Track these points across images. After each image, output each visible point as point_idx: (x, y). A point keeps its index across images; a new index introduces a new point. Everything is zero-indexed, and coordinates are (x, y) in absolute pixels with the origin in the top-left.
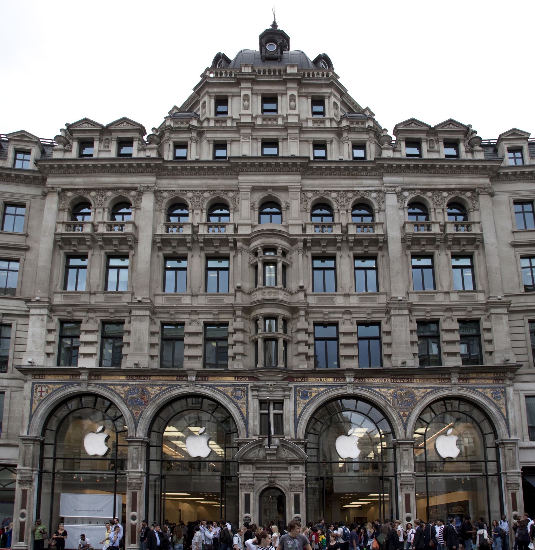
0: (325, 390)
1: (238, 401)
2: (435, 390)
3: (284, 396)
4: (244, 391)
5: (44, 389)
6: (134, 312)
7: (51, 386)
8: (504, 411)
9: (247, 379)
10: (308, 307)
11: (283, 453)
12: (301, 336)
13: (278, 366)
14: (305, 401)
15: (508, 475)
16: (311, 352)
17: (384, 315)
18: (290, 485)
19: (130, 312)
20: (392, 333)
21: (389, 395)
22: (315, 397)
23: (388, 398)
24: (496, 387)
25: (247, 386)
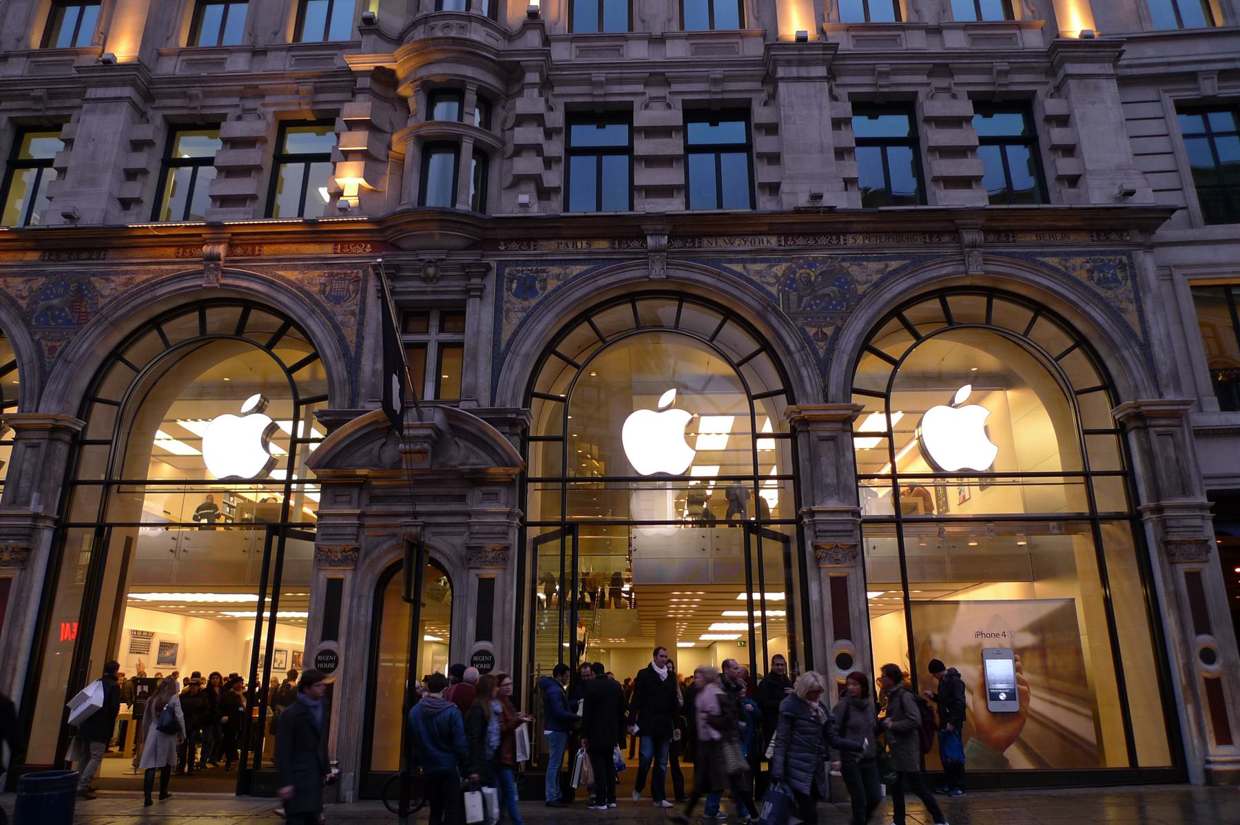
0: (586, 272)
1: (338, 309)
8: (1132, 319)
11: (453, 451)
14: (526, 304)
15: (1168, 513)
16: (553, 178)
17: (758, 85)
18: (468, 548)
20: (783, 128)
21: (772, 280)
22: (554, 291)
23: (770, 289)
24: (1102, 253)
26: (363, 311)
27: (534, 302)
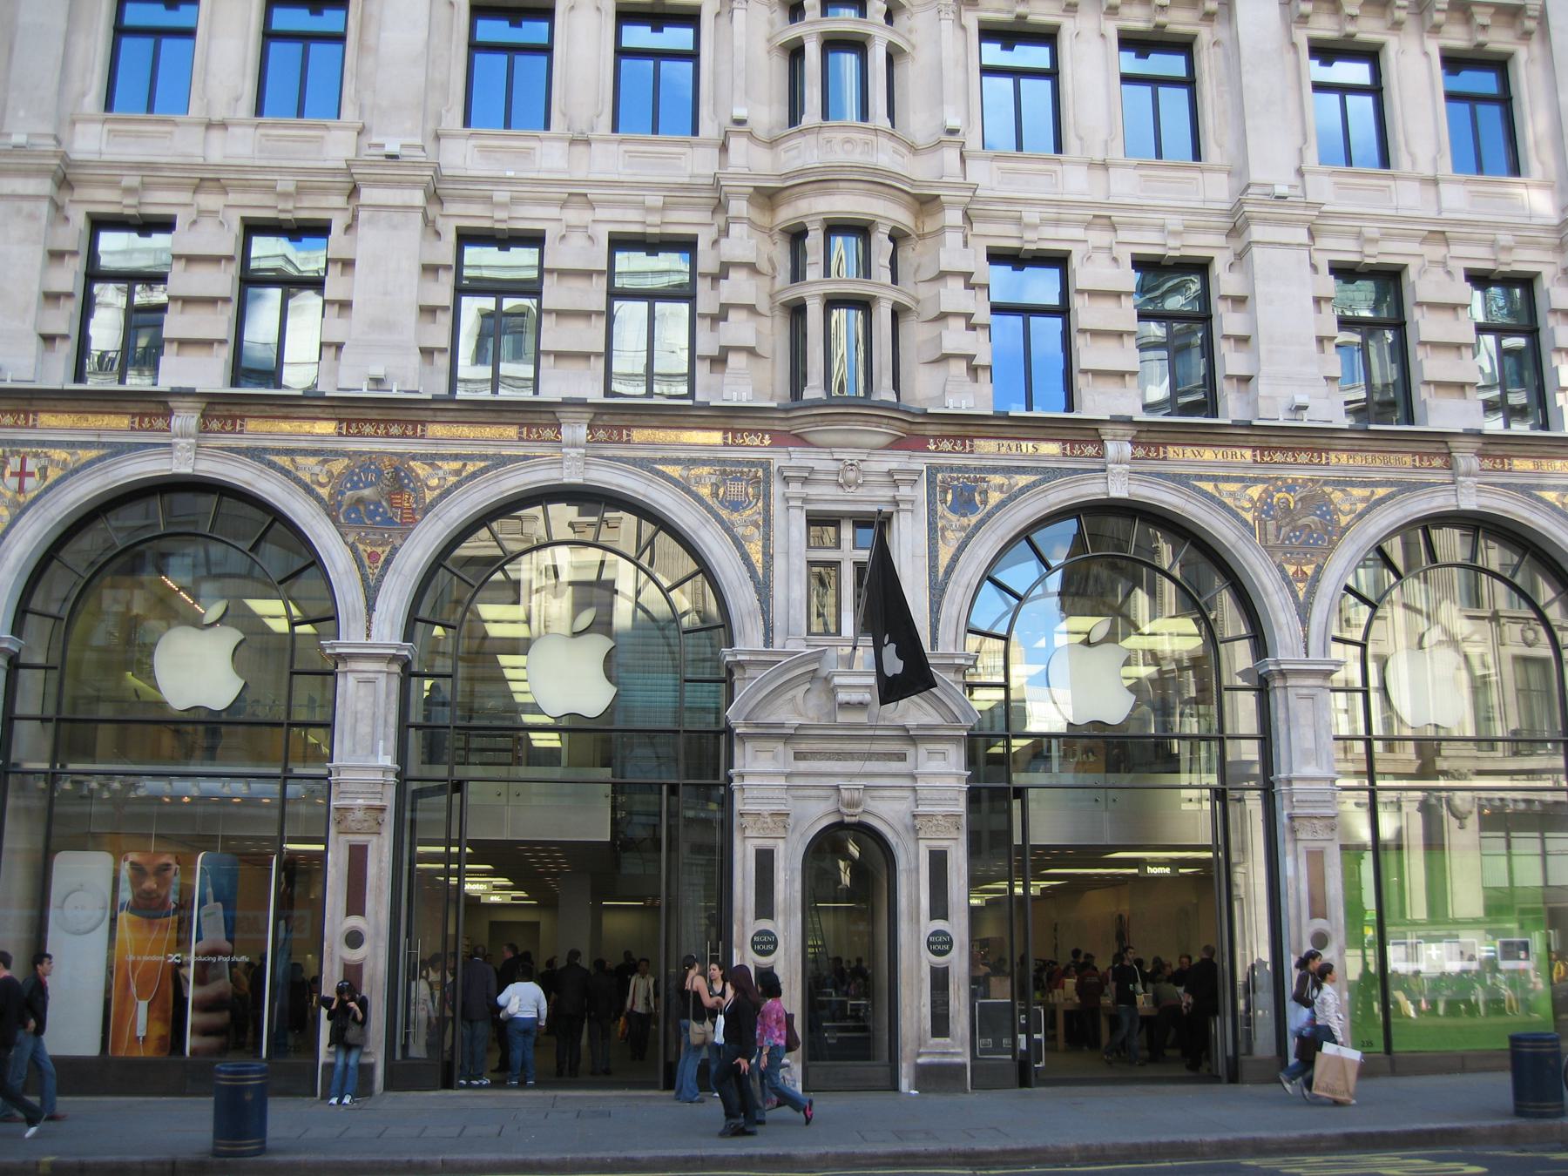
0: (1034, 484)
2: (1401, 492)
3: (896, 503)
4: (756, 481)
5: (31, 465)
6: (368, 195)
7: (59, 454)
9: (767, 442)
10: (973, 199)
12: (954, 296)
13: (875, 397)
14: (965, 521)
19: (354, 192)
21: (1248, 505)
22: (1001, 505)
25: (765, 465)
26: (767, 521)
27: (974, 519)
